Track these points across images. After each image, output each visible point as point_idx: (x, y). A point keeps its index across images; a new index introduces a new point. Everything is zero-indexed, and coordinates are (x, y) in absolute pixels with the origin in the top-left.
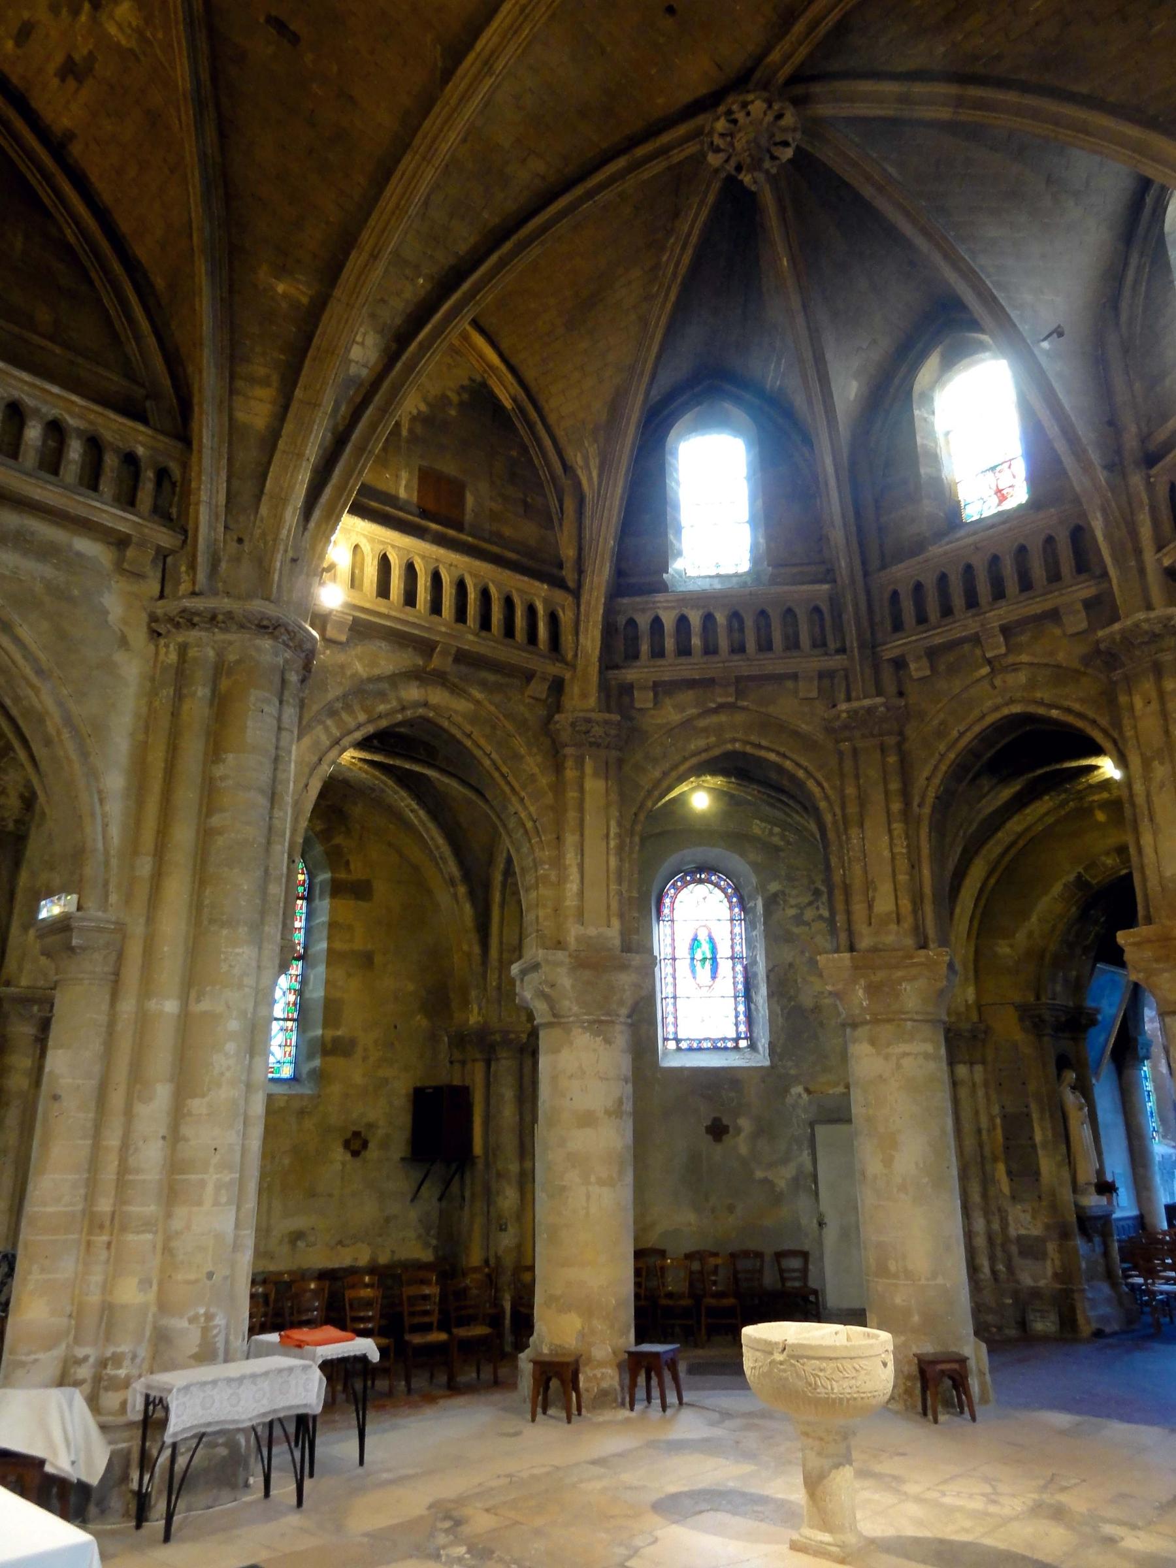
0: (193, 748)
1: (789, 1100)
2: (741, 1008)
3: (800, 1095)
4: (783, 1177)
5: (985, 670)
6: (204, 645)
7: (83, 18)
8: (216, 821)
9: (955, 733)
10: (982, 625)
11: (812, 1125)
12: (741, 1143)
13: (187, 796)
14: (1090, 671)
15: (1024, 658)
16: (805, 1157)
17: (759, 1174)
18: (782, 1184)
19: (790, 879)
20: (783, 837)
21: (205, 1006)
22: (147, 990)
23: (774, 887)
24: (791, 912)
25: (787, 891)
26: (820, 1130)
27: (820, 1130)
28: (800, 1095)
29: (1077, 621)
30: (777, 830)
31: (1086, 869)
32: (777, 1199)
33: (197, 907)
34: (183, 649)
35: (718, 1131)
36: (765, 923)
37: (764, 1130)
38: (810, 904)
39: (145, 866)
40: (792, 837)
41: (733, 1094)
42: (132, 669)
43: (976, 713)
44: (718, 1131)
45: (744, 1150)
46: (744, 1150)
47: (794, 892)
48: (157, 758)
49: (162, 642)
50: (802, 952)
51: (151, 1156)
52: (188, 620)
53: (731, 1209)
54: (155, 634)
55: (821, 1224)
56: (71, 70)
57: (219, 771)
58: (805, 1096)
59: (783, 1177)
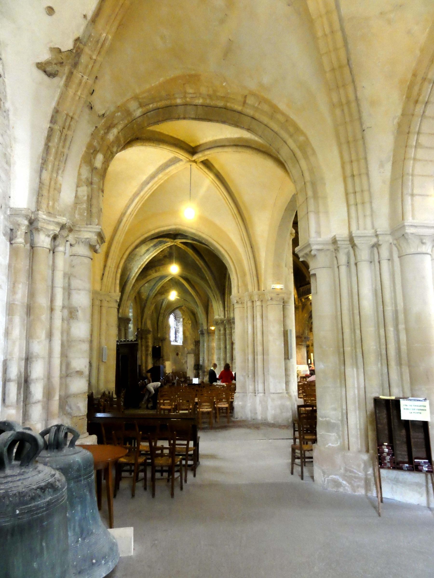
4: (184, 361)
12: (180, 356)
16: (186, 359)
18: (183, 362)
23: (184, 317)
35: (177, 354)
37: (182, 355)
45: (180, 357)
59: (184, 361)
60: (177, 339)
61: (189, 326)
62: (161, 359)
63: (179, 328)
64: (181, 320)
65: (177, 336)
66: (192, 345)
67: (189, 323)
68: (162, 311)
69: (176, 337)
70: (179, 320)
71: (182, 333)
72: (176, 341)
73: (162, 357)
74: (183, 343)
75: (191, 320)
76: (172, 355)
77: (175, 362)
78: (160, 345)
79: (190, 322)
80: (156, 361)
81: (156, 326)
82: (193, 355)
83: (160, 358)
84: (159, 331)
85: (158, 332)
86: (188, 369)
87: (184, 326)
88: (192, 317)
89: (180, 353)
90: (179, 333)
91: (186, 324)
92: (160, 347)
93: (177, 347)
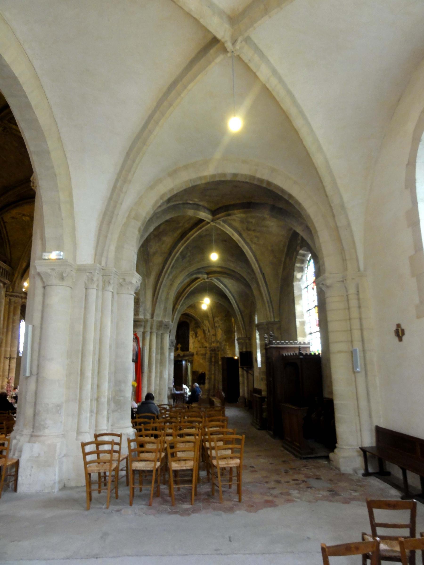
0: (12, 314)
6: (13, 299)
7: (20, 215)
8: (14, 324)
13: (11, 321)
21: (13, 349)
22: (6, 346)
33: (12, 336)
34: (10, 300)
39: (5, 330)
42: (3, 302)
48: (6, 316)
49: (7, 298)
51: (7, 367)
52: (11, 296)
54: (6, 296)
56: (13, 218)
57: (15, 318)
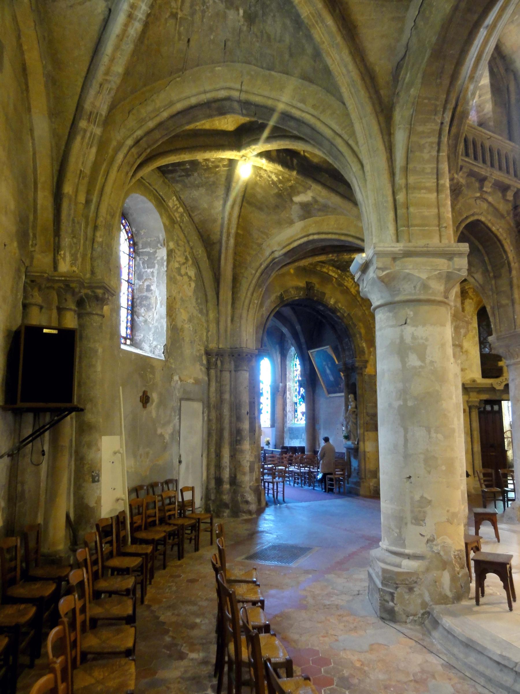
1: (173, 384)
2: (129, 317)
3: (177, 381)
5: (478, 195)
9: (465, 216)
10: (491, 175)
11: (181, 400)
14: (508, 218)
15: (490, 199)
16: (176, 420)
17: (159, 431)
19: (178, 245)
20: (182, 216)
23: (172, 245)
24: (177, 265)
25: (177, 251)
26: (183, 403)
27: (183, 402)
28: (177, 381)
29: (510, 196)
30: (181, 210)
31: (284, 292)
32: (165, 447)
35: (145, 400)
36: (167, 266)
37: (162, 403)
38: (184, 264)
40: (186, 218)
41: (151, 376)
43: (471, 212)
44: (145, 400)
45: (154, 414)
46: (154, 414)
47: (179, 253)
50: (179, 292)
53: (147, 454)
55: (180, 462)
58: (179, 382)
59: (167, 432)
60: (139, 336)
61: (189, 289)
62: (69, 425)
63: (148, 289)
64: (163, 253)
65: (139, 320)
66: (198, 366)
67: (190, 278)
68: (98, 101)
69: (133, 326)
70: (152, 256)
71: (163, 310)
72: (134, 343)
73: (80, 410)
74: (168, 350)
75: (196, 264)
76: (125, 405)
77: (140, 437)
78: (70, 321)
79: (192, 273)
80: (37, 434)
81: (44, 199)
82: (198, 406)
83: (60, 414)
84: (66, 241)
85: (57, 249)
86: (183, 465)
87: (171, 280)
88: (200, 251)
89: (155, 396)
90: (149, 308)
91: (178, 278)
92: (67, 339)
93: (144, 364)
